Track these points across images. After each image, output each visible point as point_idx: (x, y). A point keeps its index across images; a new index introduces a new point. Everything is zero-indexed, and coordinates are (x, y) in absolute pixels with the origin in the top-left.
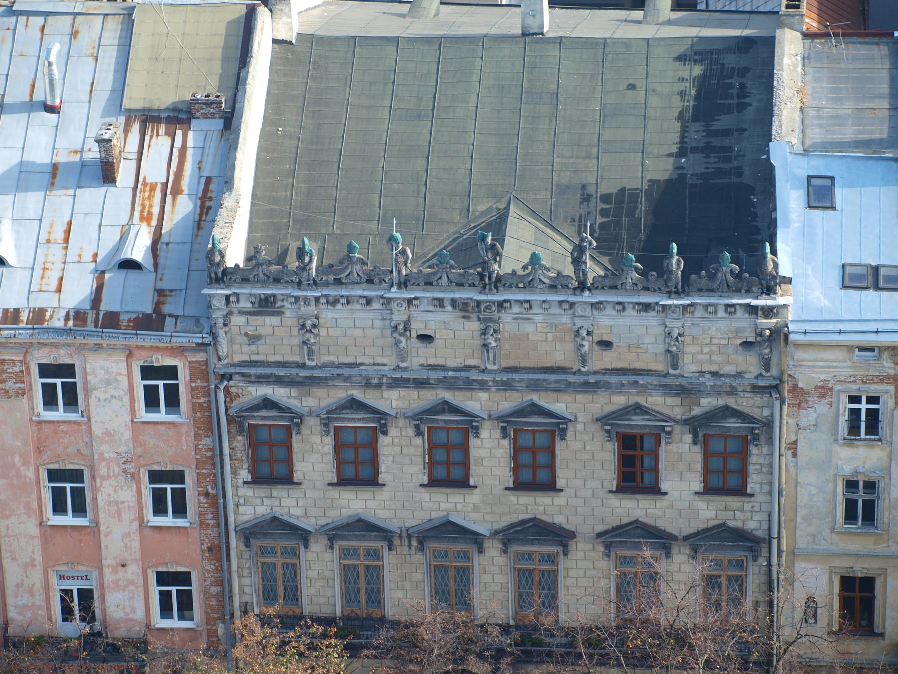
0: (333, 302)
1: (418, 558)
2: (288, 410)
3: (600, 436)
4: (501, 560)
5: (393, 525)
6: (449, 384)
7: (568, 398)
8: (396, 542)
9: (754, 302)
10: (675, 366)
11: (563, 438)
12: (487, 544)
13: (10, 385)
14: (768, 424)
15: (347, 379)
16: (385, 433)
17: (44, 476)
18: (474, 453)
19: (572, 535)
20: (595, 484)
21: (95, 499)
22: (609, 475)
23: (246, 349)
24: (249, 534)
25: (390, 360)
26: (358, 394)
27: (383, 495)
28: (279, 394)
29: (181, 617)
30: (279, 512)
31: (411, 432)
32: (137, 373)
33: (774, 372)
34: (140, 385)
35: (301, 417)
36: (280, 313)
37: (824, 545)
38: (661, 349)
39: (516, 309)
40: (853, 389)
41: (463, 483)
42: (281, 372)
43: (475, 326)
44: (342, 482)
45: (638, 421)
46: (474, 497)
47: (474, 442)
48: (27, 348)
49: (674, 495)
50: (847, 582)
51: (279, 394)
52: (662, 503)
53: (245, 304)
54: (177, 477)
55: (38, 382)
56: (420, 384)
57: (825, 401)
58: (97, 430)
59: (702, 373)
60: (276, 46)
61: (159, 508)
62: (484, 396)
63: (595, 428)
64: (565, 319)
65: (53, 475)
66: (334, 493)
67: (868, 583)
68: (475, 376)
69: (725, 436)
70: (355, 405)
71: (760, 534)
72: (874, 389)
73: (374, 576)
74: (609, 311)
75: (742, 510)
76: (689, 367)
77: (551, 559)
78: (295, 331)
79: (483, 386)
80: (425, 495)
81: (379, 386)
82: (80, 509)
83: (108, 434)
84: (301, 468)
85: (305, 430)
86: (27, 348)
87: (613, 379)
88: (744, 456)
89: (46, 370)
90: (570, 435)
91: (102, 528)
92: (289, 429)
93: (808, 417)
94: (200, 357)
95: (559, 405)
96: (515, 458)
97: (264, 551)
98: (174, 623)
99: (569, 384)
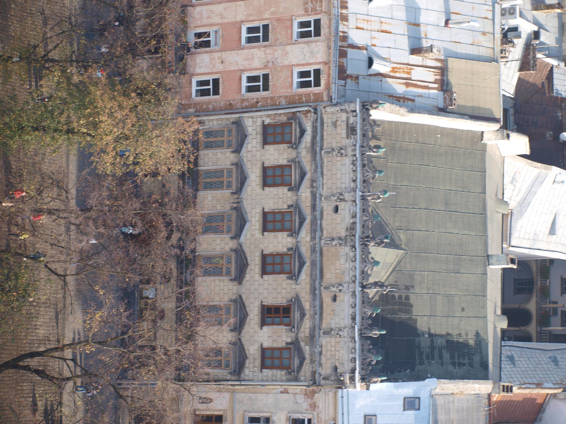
0: (354, 163)
1: (228, 207)
2: (300, 142)
3: (289, 296)
4: (227, 248)
5: (244, 195)
6: (314, 222)
7: (308, 280)
8: (235, 196)
10: (324, 333)
11: (288, 278)
12: (235, 241)
13: (310, 5)
14: (296, 379)
15: (315, 171)
16: (289, 190)
17: (266, 23)
18: (280, 234)
19: (240, 283)
20: (265, 293)
21: (254, 47)
23: (330, 120)
24: (238, 124)
25: (325, 192)
26: (308, 176)
27: (258, 190)
28: (308, 137)
29: (197, 91)
30: (249, 138)
31: (290, 203)
32: (317, 67)
33: (323, 382)
34: (311, 68)
35: (296, 148)
36: (348, 137)
37: (237, 407)
38: (333, 326)
39: (352, 254)
41: (265, 229)
42: (318, 138)
43: (343, 234)
44: (265, 169)
45: (297, 315)
46: (258, 234)
47: (285, 234)
48: (328, 13)
51: (308, 137)
52: (257, 327)
53: (352, 120)
54: (266, 88)
55: (311, 18)
56: (314, 207)
57: (308, 407)
58: (289, 48)
59: (321, 346)
60: (480, 133)
61: (251, 79)
62: (308, 239)
63: (293, 294)
64: (347, 279)
65: (266, 27)
66: (259, 165)
68: (318, 234)
69: (290, 358)
70: (303, 175)
71: (242, 376)
73: (218, 186)
74: (352, 300)
75: (254, 367)
76: (324, 340)
77: (228, 273)
78: (339, 145)
79: (313, 238)
80: (259, 210)
81: (312, 187)
82: (250, 40)
83: (287, 53)
84: (271, 149)
85: (290, 150)
86: (328, 13)
87: (317, 303)
88: (280, 367)
89: (317, 22)
90: (290, 281)
91: (240, 51)
92: (290, 142)
93: (301, 399)
94: (325, 98)
95: (304, 276)
96: (278, 254)
97: (230, 131)
98: (194, 88)
99: (315, 281)
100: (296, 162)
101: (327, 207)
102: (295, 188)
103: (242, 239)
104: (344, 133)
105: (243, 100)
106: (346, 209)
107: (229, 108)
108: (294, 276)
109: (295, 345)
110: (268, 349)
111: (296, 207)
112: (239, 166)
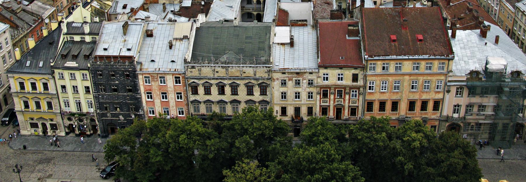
0: (203, 67)
1: (218, 105)
3: (244, 87)
4: (230, 106)
5: (214, 100)
6: (221, 79)
7: (239, 81)
9: (267, 66)
11: (239, 87)
12: (228, 103)
13: (155, 80)
14: (270, 84)
17: (161, 93)
20: (244, 94)
21: (168, 97)
22: (246, 93)
24: (192, 102)
25: (212, 76)
26: (207, 81)
27: (212, 96)
28: (195, 81)
29: (182, 115)
30: (196, 99)
31: (216, 86)
32: (174, 78)
33: (270, 76)
34: (174, 79)
35: (199, 84)
37: (278, 103)
38: (253, 73)
39: (231, 67)
40: (282, 79)
42: (196, 77)
44: (205, 94)
45: (250, 84)
46: (226, 96)
49: (256, 95)
50: (282, 108)
51: (195, 81)
52: (254, 97)
53: (190, 67)
54: (181, 93)
55: (159, 79)
56: (217, 79)
57: (278, 81)
58: (168, 86)
59: (259, 77)
62: (226, 81)
63: (244, 85)
65: (162, 93)
66: (204, 96)
67: (285, 108)
68: (225, 77)
69: (263, 86)
70: (207, 82)
71: (269, 101)
72: (285, 79)
74: (245, 67)
76: (257, 76)
78: (198, 71)
79: (226, 79)
80: (218, 96)
81: (210, 79)
82: (166, 98)
83: (170, 87)
84: (199, 92)
85: (200, 86)
86: (158, 74)
89: (160, 77)
90: (240, 86)
94: (184, 75)
95: (238, 82)
96: (232, 90)
97: (194, 104)
98: (181, 116)
99: (239, 79)
100: (203, 84)
101: (216, 75)
102: (211, 85)
103: (227, 101)
104: (194, 70)
105: (185, 101)
106: (217, 69)
107: (188, 105)
108: (238, 85)
109: (260, 85)
110: (260, 93)
111: (217, 85)
112: (205, 102)
